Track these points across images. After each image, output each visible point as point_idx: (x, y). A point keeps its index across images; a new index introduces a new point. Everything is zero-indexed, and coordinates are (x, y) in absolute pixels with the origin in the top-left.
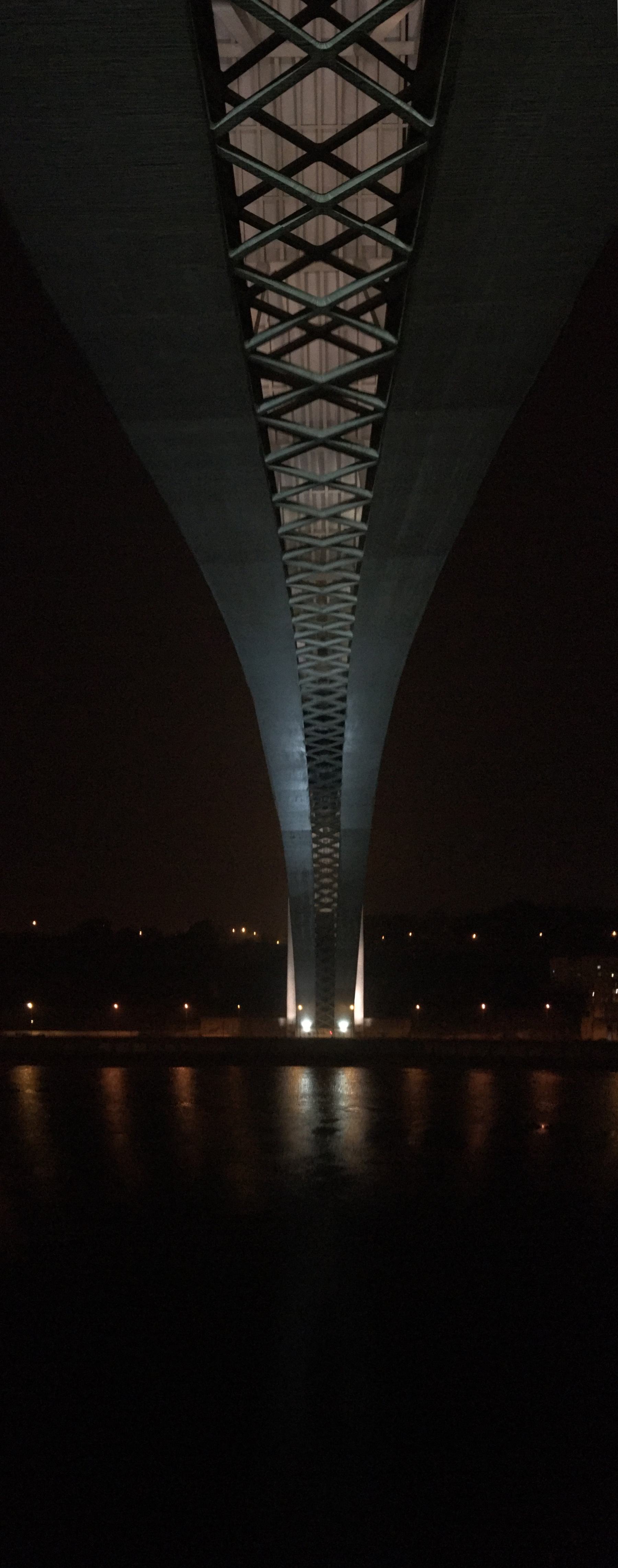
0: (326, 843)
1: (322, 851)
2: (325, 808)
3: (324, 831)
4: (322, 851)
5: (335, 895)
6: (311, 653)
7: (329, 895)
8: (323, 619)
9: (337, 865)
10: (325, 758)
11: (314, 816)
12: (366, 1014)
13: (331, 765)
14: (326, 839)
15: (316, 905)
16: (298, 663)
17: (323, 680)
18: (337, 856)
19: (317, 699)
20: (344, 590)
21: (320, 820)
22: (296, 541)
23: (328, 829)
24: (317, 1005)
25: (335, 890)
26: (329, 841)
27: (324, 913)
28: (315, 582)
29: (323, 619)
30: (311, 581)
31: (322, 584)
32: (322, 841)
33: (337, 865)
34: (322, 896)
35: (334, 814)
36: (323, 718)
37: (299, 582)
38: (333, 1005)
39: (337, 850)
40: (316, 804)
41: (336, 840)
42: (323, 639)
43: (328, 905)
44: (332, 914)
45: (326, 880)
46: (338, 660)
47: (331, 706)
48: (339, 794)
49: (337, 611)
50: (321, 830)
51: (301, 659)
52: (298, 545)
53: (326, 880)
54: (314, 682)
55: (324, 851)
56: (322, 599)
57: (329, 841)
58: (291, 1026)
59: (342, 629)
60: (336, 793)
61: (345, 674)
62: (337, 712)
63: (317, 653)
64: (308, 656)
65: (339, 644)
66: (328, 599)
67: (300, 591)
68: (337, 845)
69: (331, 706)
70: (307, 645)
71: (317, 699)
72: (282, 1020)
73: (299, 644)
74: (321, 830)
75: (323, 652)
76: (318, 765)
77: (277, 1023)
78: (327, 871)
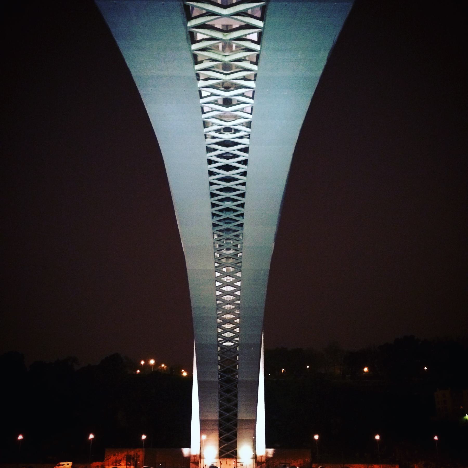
0: (228, 281)
1: (225, 289)
2: (228, 249)
3: (227, 270)
4: (225, 289)
5: (237, 330)
6: (215, 102)
7: (231, 330)
8: (226, 67)
9: (239, 302)
10: (228, 204)
11: (218, 256)
12: (268, 446)
13: (235, 211)
14: (228, 278)
15: (219, 339)
16: (203, 113)
17: (228, 130)
18: (238, 293)
19: (222, 150)
20: (249, 37)
21: (224, 260)
22: (203, 9)
23: (232, 269)
24: (220, 435)
25: (237, 325)
26: (231, 280)
27: (226, 346)
28: (219, 27)
29: (226, 67)
30: (217, 26)
31: (227, 30)
32: (225, 279)
33: (239, 302)
34: (225, 331)
35: (236, 255)
36: (227, 168)
37: (203, 26)
38: (235, 435)
39: (238, 288)
40: (220, 246)
41: (238, 279)
42: (227, 89)
43: (230, 339)
44: (234, 348)
45: (228, 316)
46: (242, 110)
47: (235, 156)
48: (241, 237)
49: (239, 60)
50: (224, 270)
51: (206, 110)
52: (204, 12)
53: (228, 316)
54: (218, 131)
55: (227, 289)
56: (227, 45)
57: (232, 279)
58: (195, 456)
59: (245, 79)
60: (237, 236)
61: (249, 125)
62: (239, 162)
63: (222, 103)
64: (211, 105)
65: (243, 95)
66: (234, 46)
67: (206, 37)
68: (239, 284)
69: (235, 156)
70: (212, 95)
71: (222, 150)
72: (186, 451)
73: (204, 94)
74: (224, 270)
75: (227, 102)
76: (221, 211)
77: (181, 453)
78: (230, 308)
